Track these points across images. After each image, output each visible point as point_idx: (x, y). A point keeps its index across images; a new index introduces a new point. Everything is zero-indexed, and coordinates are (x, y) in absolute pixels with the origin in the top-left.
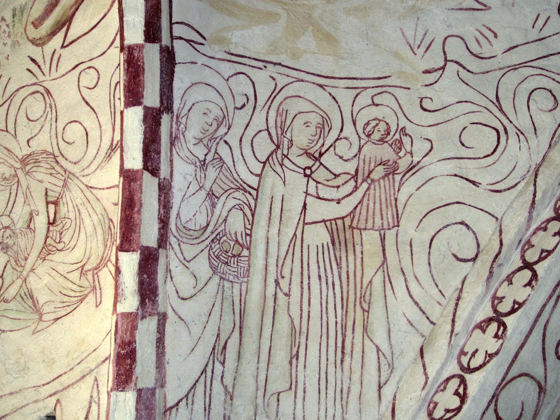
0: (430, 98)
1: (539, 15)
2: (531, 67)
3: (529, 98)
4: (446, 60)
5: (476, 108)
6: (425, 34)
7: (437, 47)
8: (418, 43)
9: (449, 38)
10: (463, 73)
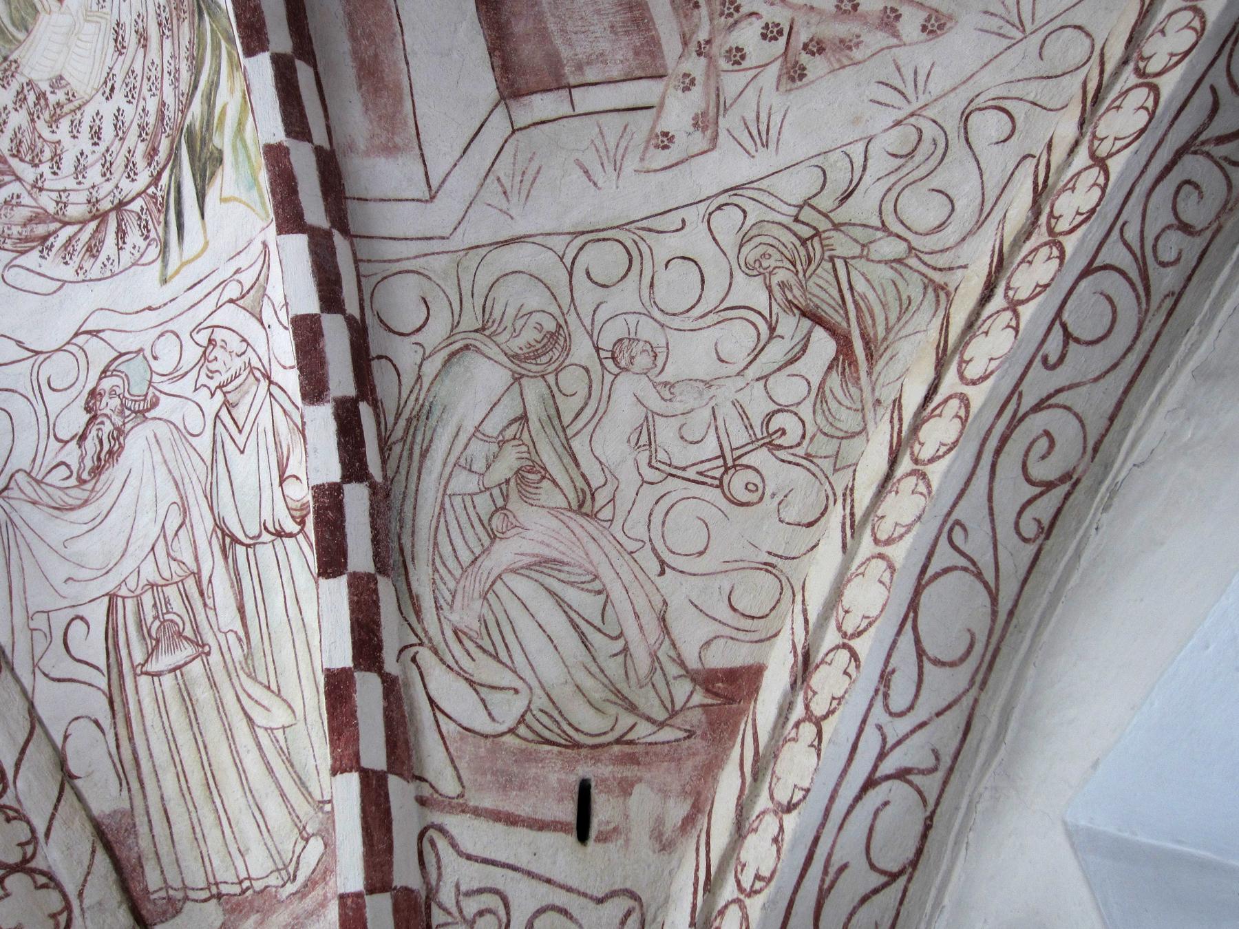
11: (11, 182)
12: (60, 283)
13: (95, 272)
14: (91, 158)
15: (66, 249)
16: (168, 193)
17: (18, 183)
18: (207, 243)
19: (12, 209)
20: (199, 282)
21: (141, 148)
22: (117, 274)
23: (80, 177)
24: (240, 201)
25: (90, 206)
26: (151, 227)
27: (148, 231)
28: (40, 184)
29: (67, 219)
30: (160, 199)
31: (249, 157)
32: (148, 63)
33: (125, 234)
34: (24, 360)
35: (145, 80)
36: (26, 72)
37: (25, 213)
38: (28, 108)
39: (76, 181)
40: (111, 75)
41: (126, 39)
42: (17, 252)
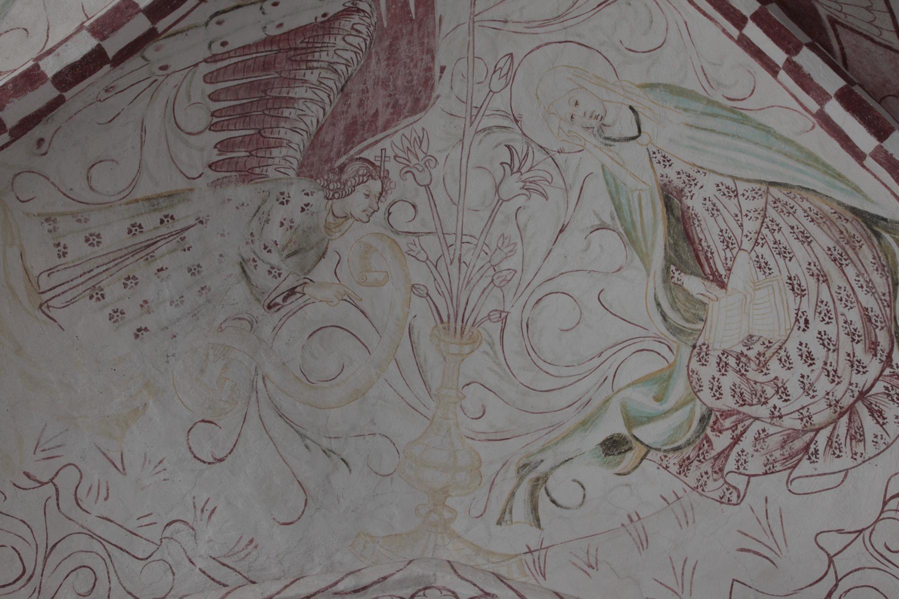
0: (5, 497)
1: (151, 514)
2: (104, 547)
3: (76, 569)
4: (51, 480)
5: (29, 538)
6: (59, 446)
7: (56, 464)
8: (46, 447)
9: (73, 467)
10: (53, 502)
11: (751, 424)
12: (844, 473)
13: (871, 450)
14: (813, 377)
15: (831, 447)
17: (757, 421)
19: (764, 442)
21: (859, 349)
22: (892, 443)
23: (811, 392)
28: (777, 413)
29: (817, 427)
32: (834, 289)
33: (881, 412)
34: (852, 542)
36: (717, 346)
37: (778, 438)
38: (734, 370)
39: (809, 397)
40: (800, 313)
41: (803, 283)
42: (789, 468)
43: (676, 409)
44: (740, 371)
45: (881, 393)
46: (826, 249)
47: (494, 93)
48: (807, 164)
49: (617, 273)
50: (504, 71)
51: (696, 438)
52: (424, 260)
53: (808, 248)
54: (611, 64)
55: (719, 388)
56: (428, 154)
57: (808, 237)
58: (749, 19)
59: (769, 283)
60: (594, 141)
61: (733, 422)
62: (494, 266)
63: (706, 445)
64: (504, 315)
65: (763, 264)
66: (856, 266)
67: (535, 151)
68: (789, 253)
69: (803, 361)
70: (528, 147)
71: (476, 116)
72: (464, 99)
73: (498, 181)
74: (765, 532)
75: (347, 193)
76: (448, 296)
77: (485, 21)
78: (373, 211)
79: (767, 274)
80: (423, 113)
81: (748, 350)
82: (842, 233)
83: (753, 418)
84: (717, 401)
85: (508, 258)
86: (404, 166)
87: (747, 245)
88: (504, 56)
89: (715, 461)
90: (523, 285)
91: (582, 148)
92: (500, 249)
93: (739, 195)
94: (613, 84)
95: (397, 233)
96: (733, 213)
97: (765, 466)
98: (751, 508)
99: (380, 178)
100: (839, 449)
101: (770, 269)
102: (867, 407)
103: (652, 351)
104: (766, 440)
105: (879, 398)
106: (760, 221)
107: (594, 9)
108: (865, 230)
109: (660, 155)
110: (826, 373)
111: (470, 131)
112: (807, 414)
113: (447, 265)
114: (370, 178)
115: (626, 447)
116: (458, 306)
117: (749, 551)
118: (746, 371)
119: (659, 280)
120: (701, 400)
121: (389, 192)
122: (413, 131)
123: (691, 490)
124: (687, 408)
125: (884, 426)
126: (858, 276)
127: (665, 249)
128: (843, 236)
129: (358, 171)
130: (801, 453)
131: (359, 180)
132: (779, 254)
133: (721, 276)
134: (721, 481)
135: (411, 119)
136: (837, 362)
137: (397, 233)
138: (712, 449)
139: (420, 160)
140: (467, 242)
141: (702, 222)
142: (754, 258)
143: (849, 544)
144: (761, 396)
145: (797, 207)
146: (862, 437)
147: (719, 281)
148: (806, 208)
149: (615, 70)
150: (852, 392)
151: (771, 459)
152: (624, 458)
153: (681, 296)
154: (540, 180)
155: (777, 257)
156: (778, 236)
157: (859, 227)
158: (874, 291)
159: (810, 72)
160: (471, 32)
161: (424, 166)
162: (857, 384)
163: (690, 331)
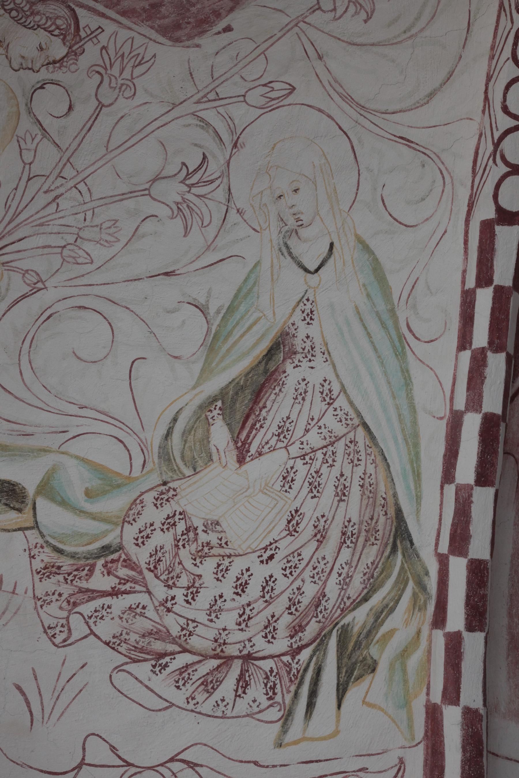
11: (141, 592)
12: (168, 704)
13: (207, 707)
14: (229, 605)
16: (306, 670)
17: (147, 595)
18: (336, 733)
19: (134, 617)
20: (317, 761)
21: (286, 619)
22: (228, 718)
23: (213, 615)
24: (386, 713)
25: (216, 644)
26: (278, 690)
27: (275, 694)
28: (169, 605)
29: (188, 647)
30: (295, 671)
31: (405, 681)
32: (319, 555)
33: (247, 685)
34: (113, 766)
35: (310, 567)
36: (183, 502)
37: (148, 625)
38: (175, 535)
40: (273, 546)
41: (302, 526)
42: (130, 658)
43: (94, 517)
44: (178, 541)
45: (264, 671)
46: (347, 519)
47: (245, 101)
48: (406, 440)
49: (171, 358)
50: (273, 95)
51: (84, 558)
52: (26, 161)
53: (336, 503)
54: (357, 194)
55: (148, 537)
56: (134, 81)
57: (344, 495)
58: (493, 286)
59: (277, 498)
60: (275, 236)
61: (127, 576)
62: (79, 237)
63: (85, 572)
64: (40, 285)
65: (289, 478)
66: (353, 555)
67: (221, 186)
68: (318, 492)
69: (234, 585)
70: (219, 177)
71: (209, 101)
72: (216, 76)
73: (164, 174)
74: (54, 692)
75: (26, 24)
76: (12, 215)
77: (306, 35)
78: (30, 66)
79: (284, 489)
80: (170, 43)
81: (203, 531)
82: (372, 519)
83: (148, 589)
84: (134, 546)
85: (98, 245)
86: (103, 64)
87: (294, 450)
88: (287, 83)
89: (78, 593)
90: (85, 281)
91: (259, 230)
92: (101, 229)
93: (332, 406)
94: (340, 210)
95: (30, 111)
96: (312, 414)
97: (114, 637)
98: (65, 660)
99: (70, 48)
100: (185, 682)
101: (290, 487)
102: (241, 671)
103: (128, 450)
104: (137, 617)
105: (258, 672)
106: (324, 443)
107: (395, 136)
108: (390, 535)
109: (311, 307)
110: (241, 612)
111: (190, 107)
112: (191, 629)
113: (40, 189)
114: (62, 37)
115: (17, 506)
116: (9, 233)
117: (23, 694)
118: (184, 546)
119: (197, 401)
120: (122, 531)
121: (64, 69)
122: (144, 47)
123: (32, 596)
124: (104, 527)
125: (238, 698)
126: (346, 564)
127: (230, 383)
128: (369, 522)
129: (58, 17)
130: (152, 655)
131: (51, 26)
132: (310, 484)
133: (248, 451)
134: (65, 614)
135: (153, 34)
136: (258, 613)
137: (30, 111)
138: (87, 580)
139: (122, 77)
140: (80, 192)
141: (282, 395)
142: (288, 466)
143: (109, 766)
144: (172, 578)
145: (363, 463)
146: (212, 691)
147: (242, 453)
148: (368, 472)
149: (354, 201)
150: (244, 647)
151: (124, 636)
152: (6, 512)
153: (200, 433)
154: (197, 214)
155: (306, 484)
156: (324, 470)
157: (388, 528)
158: (345, 587)
159: (488, 376)
160: (285, 30)
161: (119, 85)
162: (254, 645)
163: (176, 468)
